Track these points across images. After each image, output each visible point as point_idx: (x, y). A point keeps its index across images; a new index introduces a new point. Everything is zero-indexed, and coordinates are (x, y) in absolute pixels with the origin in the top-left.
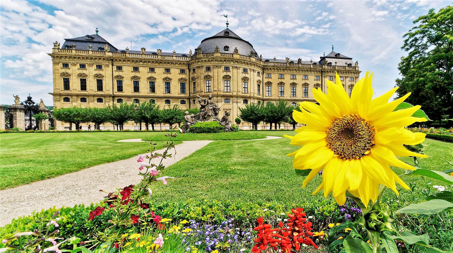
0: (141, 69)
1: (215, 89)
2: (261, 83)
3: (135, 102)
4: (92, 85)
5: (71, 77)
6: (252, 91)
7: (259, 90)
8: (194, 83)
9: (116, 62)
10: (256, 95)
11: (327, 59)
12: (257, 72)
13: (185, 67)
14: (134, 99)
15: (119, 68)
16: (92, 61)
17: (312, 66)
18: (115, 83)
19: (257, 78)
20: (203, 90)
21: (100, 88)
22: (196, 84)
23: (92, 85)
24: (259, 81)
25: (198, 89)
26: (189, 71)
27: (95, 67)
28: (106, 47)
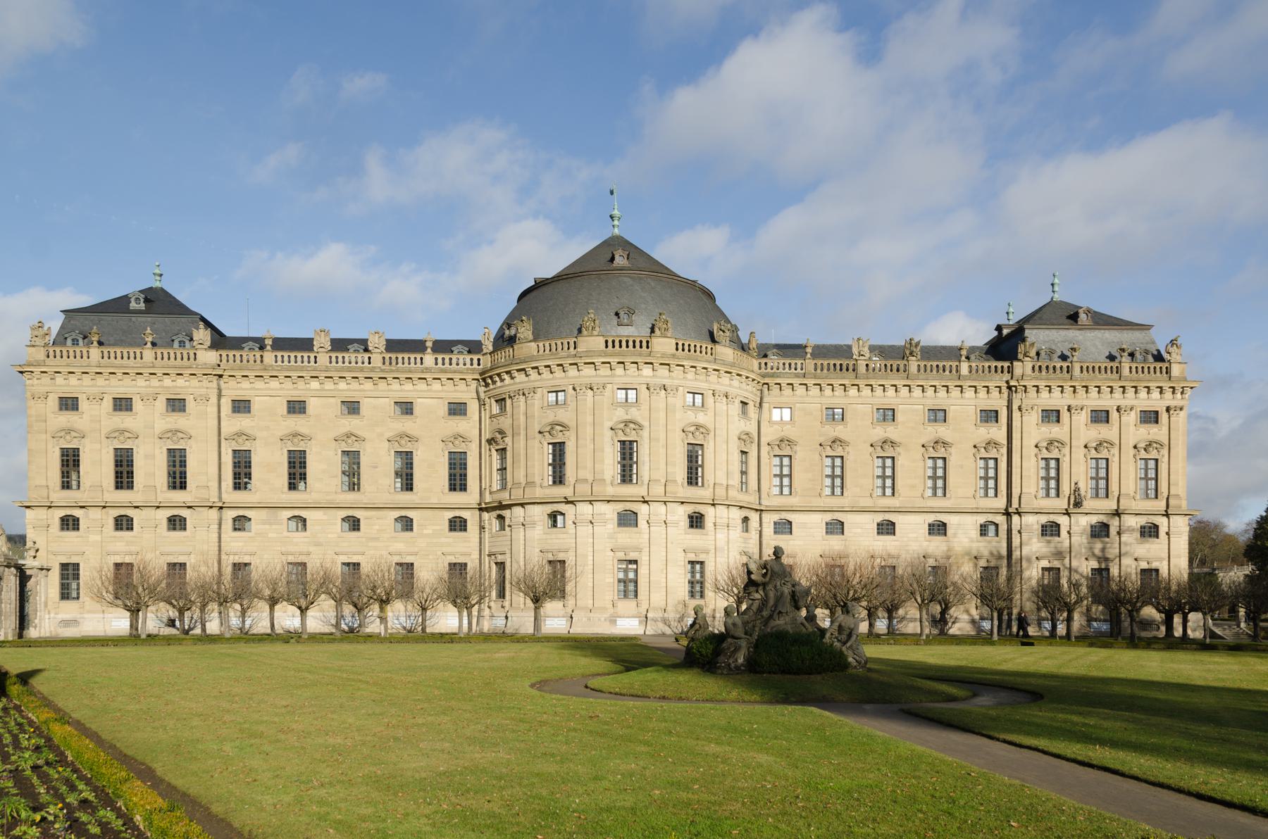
0: (313, 405)
1: (582, 474)
2: (755, 446)
3: (293, 524)
4: (151, 469)
5: (86, 441)
6: (721, 479)
7: (743, 473)
8: (503, 451)
9: (232, 382)
10: (733, 493)
11: (1031, 334)
12: (737, 402)
13: (466, 393)
14: (290, 513)
15: (241, 406)
16: (154, 382)
17: (964, 367)
18: (228, 460)
19: (741, 425)
20: (537, 480)
21: (178, 480)
22: (509, 454)
23: (151, 469)
24: (744, 437)
25: (517, 474)
26: (482, 404)
27: (161, 404)
28: (202, 335)
